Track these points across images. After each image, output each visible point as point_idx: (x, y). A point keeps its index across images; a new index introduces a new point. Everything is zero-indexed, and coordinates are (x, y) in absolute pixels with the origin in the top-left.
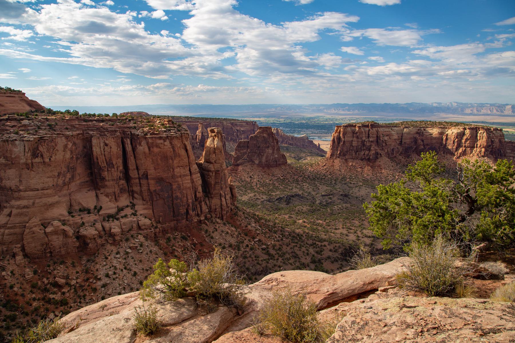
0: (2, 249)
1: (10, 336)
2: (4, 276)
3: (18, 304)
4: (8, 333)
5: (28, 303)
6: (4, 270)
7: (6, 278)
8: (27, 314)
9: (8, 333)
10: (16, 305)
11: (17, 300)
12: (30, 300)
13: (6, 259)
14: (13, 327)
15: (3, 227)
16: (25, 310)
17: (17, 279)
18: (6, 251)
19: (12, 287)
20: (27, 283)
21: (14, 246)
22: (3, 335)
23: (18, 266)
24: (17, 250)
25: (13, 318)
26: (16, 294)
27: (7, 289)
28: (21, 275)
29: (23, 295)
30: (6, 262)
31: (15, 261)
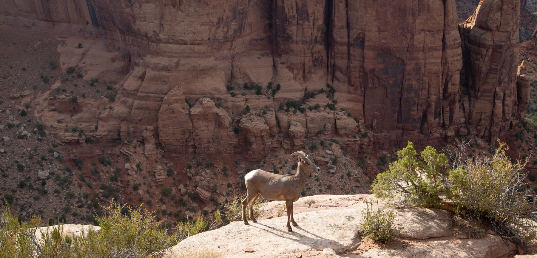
0: (128, 128)
2: (127, 169)
6: (128, 160)
7: (130, 173)
13: (132, 145)
17: (144, 178)
18: (134, 132)
19: (136, 188)
20: (157, 186)
21: (144, 127)
23: (147, 158)
27: (129, 190)
28: (149, 172)
30: (132, 150)
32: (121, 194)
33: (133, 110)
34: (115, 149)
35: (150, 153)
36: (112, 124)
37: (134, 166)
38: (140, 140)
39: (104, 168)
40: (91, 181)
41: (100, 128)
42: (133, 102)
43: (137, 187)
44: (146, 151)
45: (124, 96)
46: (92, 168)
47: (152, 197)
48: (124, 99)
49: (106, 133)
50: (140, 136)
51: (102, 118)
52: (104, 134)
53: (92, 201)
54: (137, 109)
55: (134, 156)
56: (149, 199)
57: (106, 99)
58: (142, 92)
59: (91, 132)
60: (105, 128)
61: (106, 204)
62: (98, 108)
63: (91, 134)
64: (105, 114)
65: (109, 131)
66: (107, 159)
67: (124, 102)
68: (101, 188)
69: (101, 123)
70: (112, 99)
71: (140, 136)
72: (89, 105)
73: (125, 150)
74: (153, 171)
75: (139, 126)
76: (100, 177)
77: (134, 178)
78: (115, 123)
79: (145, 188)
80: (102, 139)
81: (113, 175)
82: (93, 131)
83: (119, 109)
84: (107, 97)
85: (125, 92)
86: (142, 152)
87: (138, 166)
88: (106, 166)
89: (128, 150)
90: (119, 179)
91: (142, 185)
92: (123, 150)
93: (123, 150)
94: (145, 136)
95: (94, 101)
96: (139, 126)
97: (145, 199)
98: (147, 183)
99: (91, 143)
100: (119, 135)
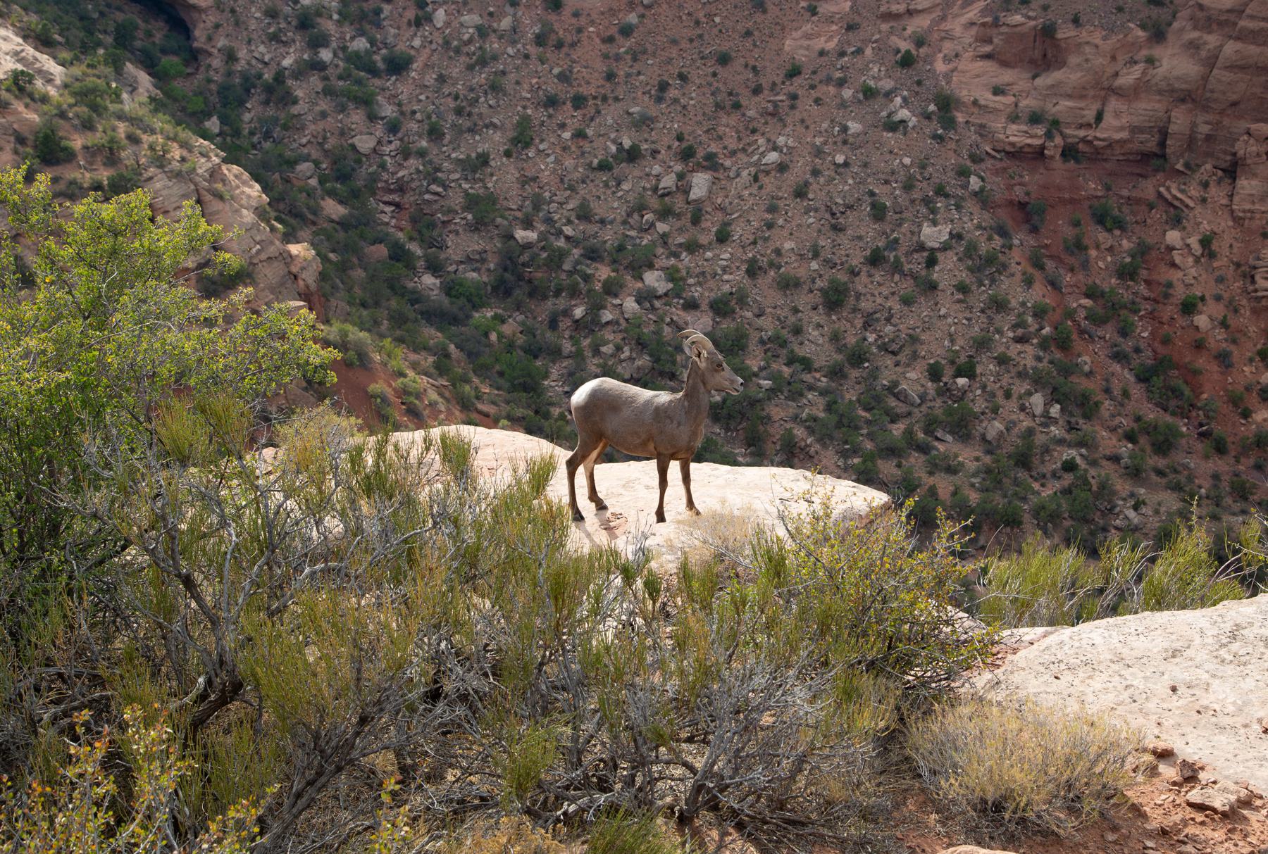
0: (1194, 125)
1: (1136, 508)
2: (1171, 249)
3: (1197, 392)
4: (1132, 495)
5: (1235, 401)
6: (1177, 223)
7: (1178, 260)
8: (1220, 448)
9: (1132, 495)
10: (1187, 392)
11: (1196, 373)
12: (1248, 389)
13: (1197, 176)
14: (1154, 477)
15: (1221, 24)
16: (1218, 429)
17: (1220, 280)
18: (1209, 138)
19: (1189, 308)
20: (1255, 311)
21: (1243, 125)
22: (1114, 493)
23: (1238, 221)
24: (1253, 148)
25: (1164, 445)
26: (1199, 346)
27: (1169, 311)
28: (1238, 265)
29: (1223, 359)
30: (1195, 191)
31: (1231, 196)
32: (1141, 318)
33: (1215, 71)
34: (1143, 183)
35: (1248, 206)
36: (1148, 108)
37: (1194, 241)
38: (1223, 166)
39: (1102, 236)
40: (1062, 271)
41: (1108, 119)
42: (1222, 46)
43: (1194, 305)
44: (1236, 199)
45: (1195, 28)
46: (1069, 232)
47: (1234, 342)
48: (1195, 34)
49: (1124, 135)
50: (1225, 152)
51: (1120, 88)
52: (1117, 136)
53: (1056, 328)
54: (1231, 68)
55: (1199, 209)
56: (1224, 345)
57: (1140, 33)
58: (1252, 17)
59: (1081, 126)
60: (1124, 121)
61: (1093, 341)
62: (1114, 58)
63: (1082, 133)
64: (1128, 78)
65: (1135, 130)
66: (1116, 212)
67: (1193, 46)
68: (1088, 296)
69: (1114, 104)
70: (1158, 35)
71: (1225, 152)
72: (1087, 49)
73: (1173, 190)
74: (1252, 262)
75: (1226, 122)
76: (1087, 261)
77: (1188, 276)
78: (1157, 106)
79: (1217, 310)
80: (1109, 151)
81: (1128, 260)
82: (1089, 126)
83: (1174, 64)
84: (1143, 27)
85: (1200, 14)
86: (1225, 201)
87: (1205, 242)
88: (1109, 230)
89: (1182, 191)
90: (1144, 273)
91: (1210, 302)
92: (1168, 189)
93: (1168, 189)
94: (1241, 153)
95: (1105, 38)
96: (1226, 122)
97: (1212, 344)
98: (1226, 296)
99: (1077, 161)
100: (1162, 144)
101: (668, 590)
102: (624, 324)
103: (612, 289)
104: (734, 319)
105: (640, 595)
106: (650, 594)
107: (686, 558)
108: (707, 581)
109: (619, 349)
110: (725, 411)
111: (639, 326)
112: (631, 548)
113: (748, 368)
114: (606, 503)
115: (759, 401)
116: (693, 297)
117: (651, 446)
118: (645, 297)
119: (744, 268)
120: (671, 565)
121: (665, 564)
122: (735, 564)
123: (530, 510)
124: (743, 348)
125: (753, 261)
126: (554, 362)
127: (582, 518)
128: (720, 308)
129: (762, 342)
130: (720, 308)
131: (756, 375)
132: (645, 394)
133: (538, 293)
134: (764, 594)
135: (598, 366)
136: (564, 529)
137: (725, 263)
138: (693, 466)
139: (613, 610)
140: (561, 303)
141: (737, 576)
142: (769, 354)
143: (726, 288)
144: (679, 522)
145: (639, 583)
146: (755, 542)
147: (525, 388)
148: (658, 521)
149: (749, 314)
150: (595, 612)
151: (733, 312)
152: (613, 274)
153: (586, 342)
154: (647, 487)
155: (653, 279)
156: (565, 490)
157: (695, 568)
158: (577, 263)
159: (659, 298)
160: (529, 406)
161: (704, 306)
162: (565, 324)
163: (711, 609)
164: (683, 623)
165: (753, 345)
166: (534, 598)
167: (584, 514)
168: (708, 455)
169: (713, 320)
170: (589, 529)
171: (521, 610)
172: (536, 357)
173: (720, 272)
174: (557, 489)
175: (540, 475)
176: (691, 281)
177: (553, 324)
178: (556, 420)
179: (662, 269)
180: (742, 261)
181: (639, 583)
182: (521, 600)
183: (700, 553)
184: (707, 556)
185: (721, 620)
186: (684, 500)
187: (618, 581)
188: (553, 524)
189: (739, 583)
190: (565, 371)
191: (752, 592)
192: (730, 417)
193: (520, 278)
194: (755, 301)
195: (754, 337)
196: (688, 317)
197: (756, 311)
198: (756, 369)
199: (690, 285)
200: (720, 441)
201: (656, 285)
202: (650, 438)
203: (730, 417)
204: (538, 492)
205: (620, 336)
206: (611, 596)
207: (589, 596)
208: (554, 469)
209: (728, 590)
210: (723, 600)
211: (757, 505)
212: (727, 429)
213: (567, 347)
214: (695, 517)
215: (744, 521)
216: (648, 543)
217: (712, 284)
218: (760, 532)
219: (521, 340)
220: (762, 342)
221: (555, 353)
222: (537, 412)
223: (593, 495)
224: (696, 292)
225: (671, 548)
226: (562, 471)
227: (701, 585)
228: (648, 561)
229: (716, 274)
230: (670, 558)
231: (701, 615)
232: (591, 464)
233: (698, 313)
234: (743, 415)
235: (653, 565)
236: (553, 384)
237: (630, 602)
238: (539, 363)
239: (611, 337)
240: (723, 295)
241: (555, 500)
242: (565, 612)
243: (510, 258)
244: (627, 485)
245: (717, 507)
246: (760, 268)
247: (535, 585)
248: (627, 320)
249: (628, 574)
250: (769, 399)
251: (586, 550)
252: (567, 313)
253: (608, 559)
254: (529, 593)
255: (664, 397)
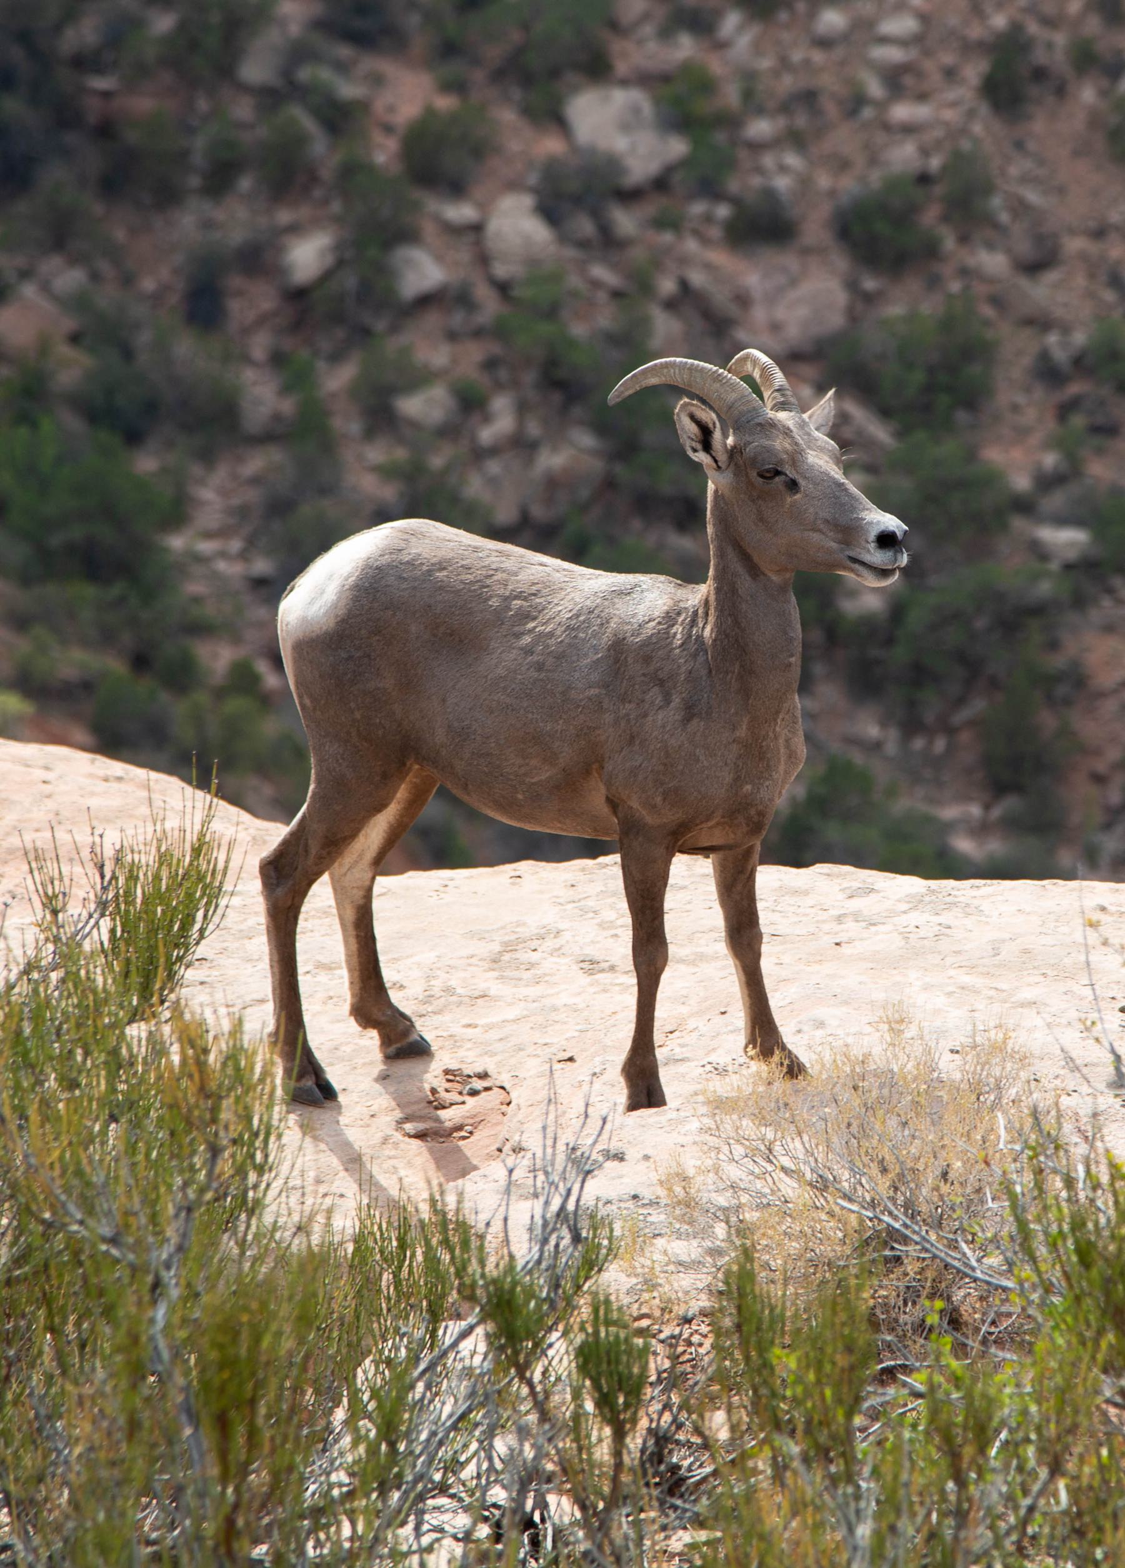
101: (672, 1380)
102: (490, 305)
103: (440, 161)
104: (934, 282)
105: (562, 1401)
106: (604, 1401)
107: (747, 1254)
108: (830, 1341)
109: (471, 403)
110: (900, 655)
111: (552, 312)
112: (524, 1213)
113: (991, 479)
114: (426, 1029)
115: (1038, 610)
116: (769, 194)
117: (596, 799)
118: (578, 194)
119: (974, 71)
120: (685, 1281)
121: (664, 1277)
122: (942, 1279)
123: (116, 1063)
124: (972, 398)
125: (1008, 49)
126: (207, 456)
127: (327, 1093)
128: (881, 237)
129: (1049, 373)
130: (881, 237)
131: (1024, 506)
132: (575, 589)
133: (136, 176)
134: (1063, 1393)
135: (386, 472)
136: (252, 1143)
137: (894, 54)
138: (770, 881)
139: (454, 1466)
140: (236, 218)
141: (955, 1321)
142: (1078, 421)
143: (904, 156)
144: (719, 1105)
145: (559, 1355)
146: (1023, 1183)
147: (94, 564)
148: (634, 1105)
149: (993, 262)
150: (380, 1474)
151: (931, 251)
152: (445, 103)
153: (337, 379)
154: (591, 965)
155: (608, 122)
156: (259, 980)
157: (785, 1294)
158: (299, 53)
159: (630, 196)
160: (107, 638)
161: (815, 228)
162: (250, 303)
163: (849, 1457)
164: (734, 1515)
165: (1016, 396)
166: (133, 1426)
167: (334, 1076)
168: (832, 832)
169: (852, 286)
170: (355, 1136)
171: (78, 1474)
172: (134, 437)
173: (875, 88)
174: (226, 980)
175: (156, 925)
176: (761, 128)
177: (204, 304)
178: (220, 693)
179: (645, 79)
180: (968, 48)
181: (559, 1355)
182: (78, 1435)
183: (803, 1232)
184: (833, 1239)
185: (891, 1504)
186: (739, 1017)
187: (474, 1348)
188: (204, 1120)
189: (960, 1349)
190: (252, 495)
191: (1013, 1387)
192: (920, 675)
193: (65, 115)
194: (1020, 208)
195: (1017, 352)
196: (752, 274)
197: (1025, 248)
198: (1022, 482)
199: (757, 147)
200: (881, 772)
201: (620, 144)
202: (591, 763)
203: (920, 675)
204: (145, 991)
205: (474, 353)
206: (447, 1408)
207: (356, 1411)
208: (213, 894)
209: (917, 1380)
210: (897, 1416)
211: (1032, 1034)
212: (911, 726)
213: (262, 396)
214: (781, 1086)
215: (980, 1094)
216: (595, 1189)
217: (843, 139)
218: (1042, 1143)
219: (72, 369)
220: (1049, 373)
221: (214, 424)
222: (140, 662)
223: (372, 1001)
224: (783, 174)
225: (688, 1209)
226: (245, 902)
227: (806, 1363)
228: (591, 1264)
229: (856, 102)
230: (685, 1249)
231: (810, 1482)
232: (362, 873)
233: (789, 260)
234: (972, 668)
235: (615, 1280)
236: (206, 547)
237: (523, 1432)
238: (146, 462)
239: (436, 355)
240: (893, 185)
241: (218, 1023)
242: (258, 1478)
243: (25, 37)
244: (508, 956)
245: (873, 1044)
246: (1040, 74)
247: (137, 1372)
248: (503, 288)
249: (514, 1322)
250: (1079, 602)
251: (345, 1223)
252: (259, 259)
253: (431, 1260)
254: (112, 1407)
255: (649, 599)
